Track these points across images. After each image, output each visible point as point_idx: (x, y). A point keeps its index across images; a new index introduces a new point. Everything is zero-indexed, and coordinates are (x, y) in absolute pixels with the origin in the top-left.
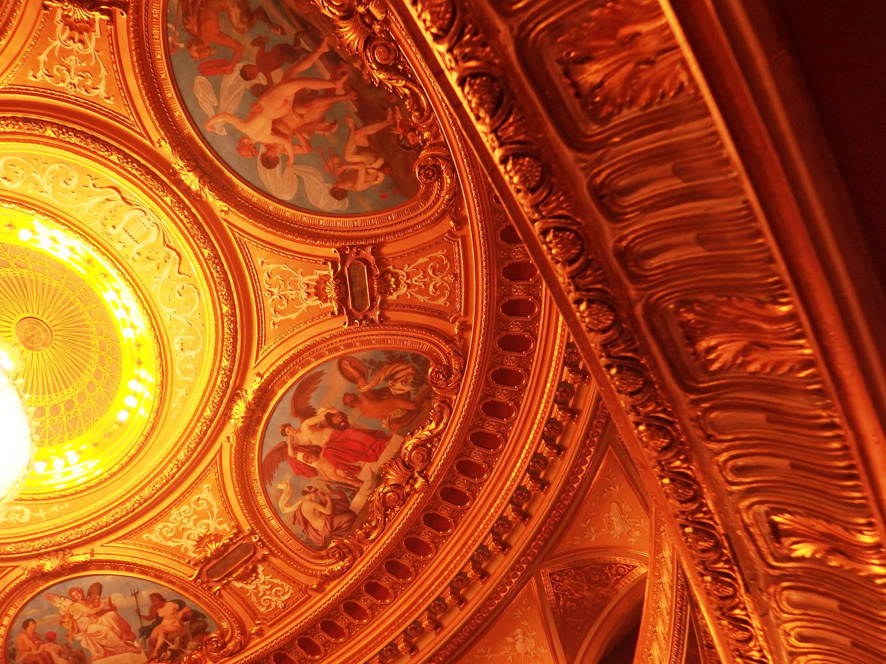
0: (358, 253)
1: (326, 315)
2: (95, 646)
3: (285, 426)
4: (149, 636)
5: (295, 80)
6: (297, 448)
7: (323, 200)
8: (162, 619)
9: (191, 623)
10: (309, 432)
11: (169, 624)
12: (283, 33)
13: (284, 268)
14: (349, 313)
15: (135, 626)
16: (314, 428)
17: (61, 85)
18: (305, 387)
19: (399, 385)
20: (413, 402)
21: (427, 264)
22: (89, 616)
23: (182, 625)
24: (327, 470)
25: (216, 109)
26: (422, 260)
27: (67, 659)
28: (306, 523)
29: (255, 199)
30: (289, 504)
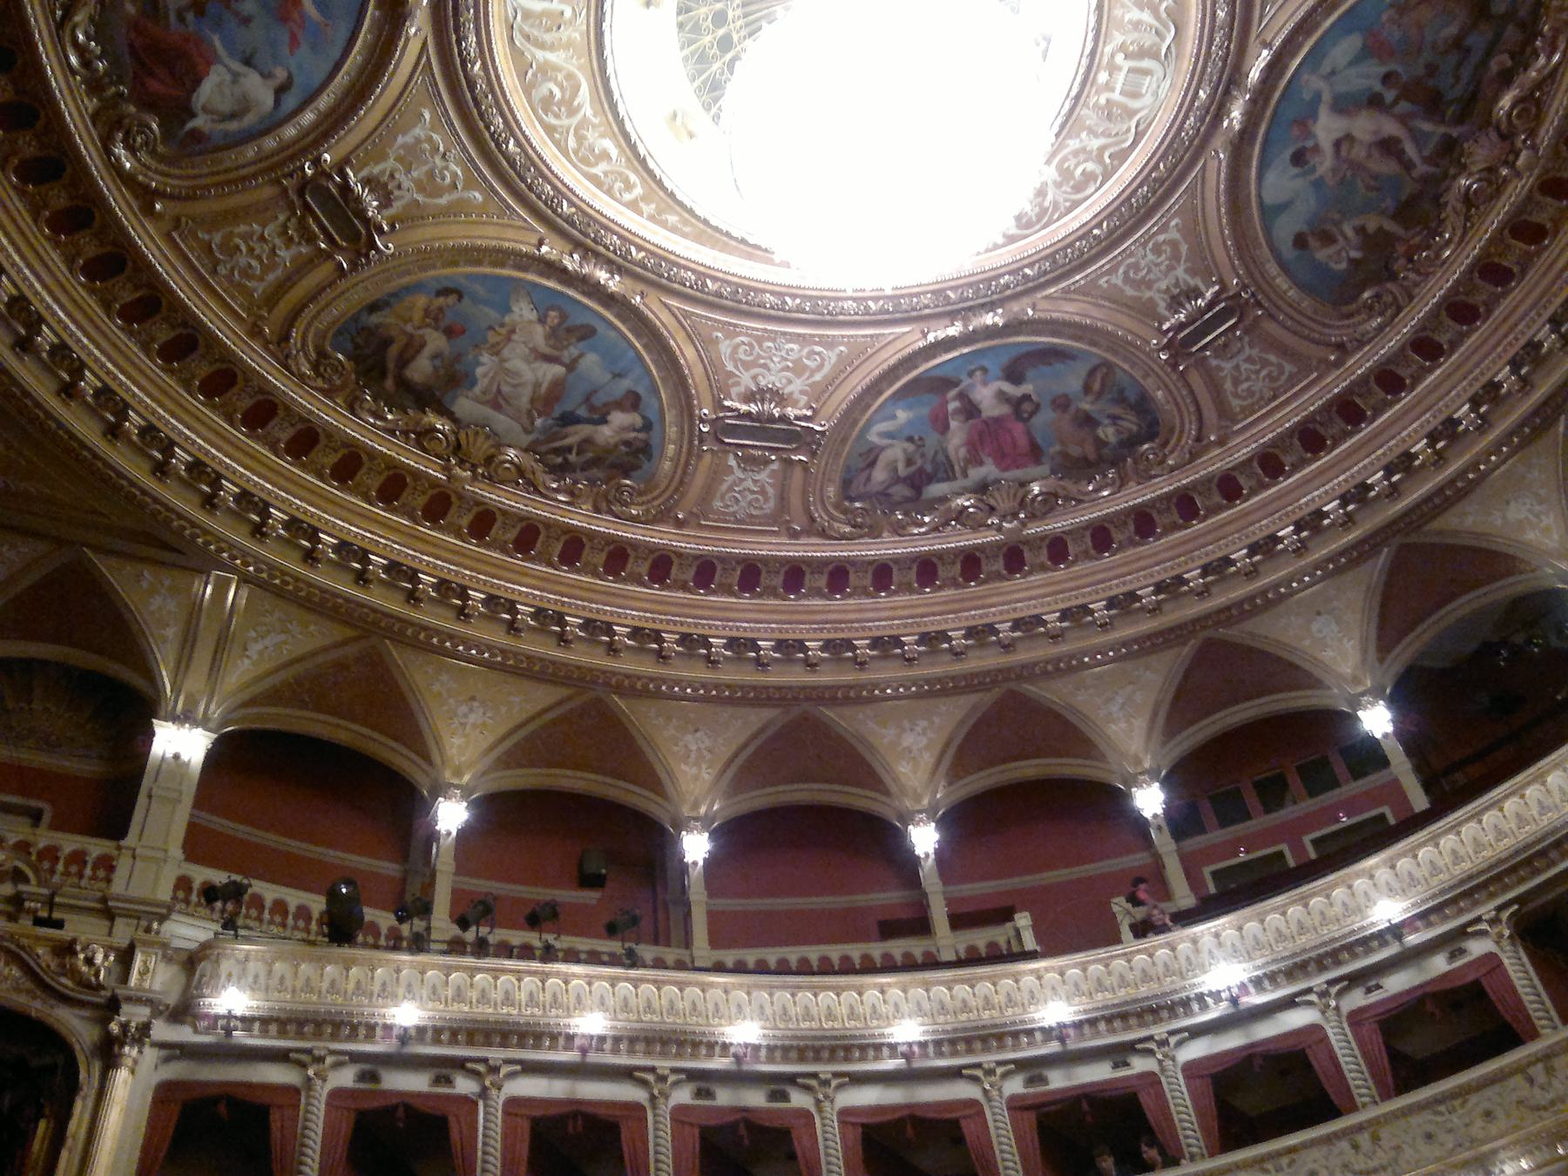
2: (491, 383)
3: (984, 370)
6: (962, 396)
12: (1452, 86)
14: (1171, 340)
16: (1002, 396)
21: (1271, 364)
23: (616, 446)
24: (957, 438)
26: (1272, 358)
28: (872, 464)
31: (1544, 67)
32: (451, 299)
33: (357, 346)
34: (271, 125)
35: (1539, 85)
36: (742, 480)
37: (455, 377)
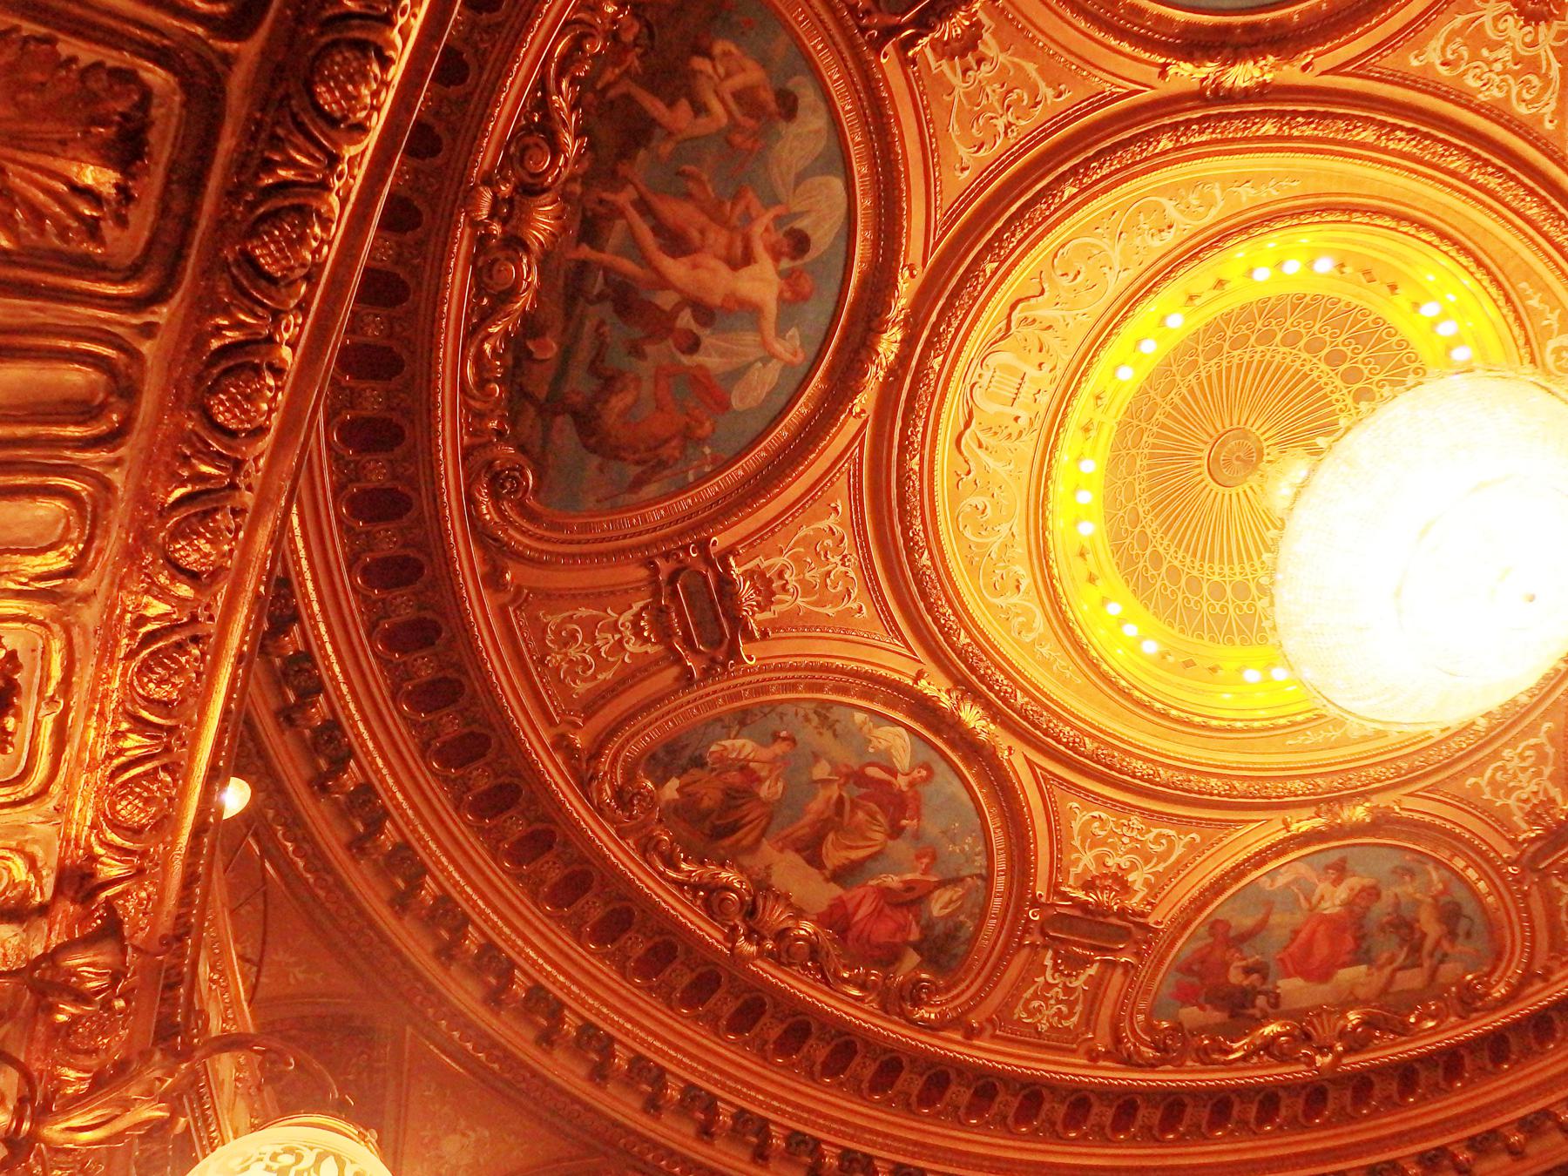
0: (868, 13)
1: (1003, 9)
5: (656, 270)
7: (812, 122)
12: (602, 323)
13: (955, 130)
17: (852, 574)
25: (765, 361)
29: (868, 235)
31: (482, 342)
35: (487, 317)
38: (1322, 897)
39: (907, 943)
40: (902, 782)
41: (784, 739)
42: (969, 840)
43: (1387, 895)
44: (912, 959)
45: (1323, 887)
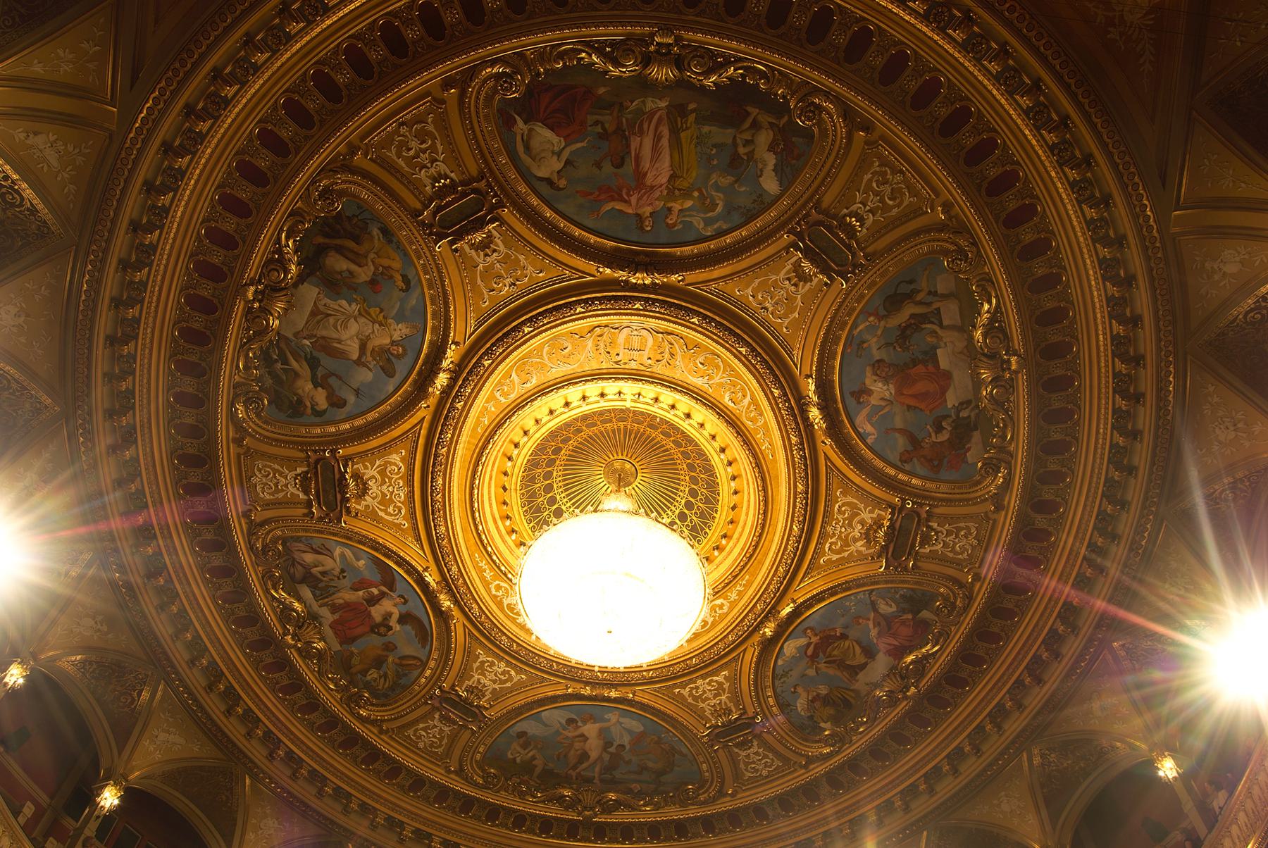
2: (334, 310)
3: (406, 602)
4: (306, 360)
5: (597, 760)
6: (383, 595)
8: (316, 387)
9: (291, 402)
10: (388, 610)
11: (305, 386)
15: (327, 362)
16: (388, 616)
18: (423, 635)
19: (375, 675)
20: (356, 674)
22: (368, 338)
23: (296, 394)
25: (621, 723)
27: (340, 273)
30: (343, 555)
32: (401, 284)
33: (349, 219)
34: (526, 175)
36: (286, 477)
37: (334, 285)
38: (882, 399)
39: (913, 619)
40: (814, 640)
41: (795, 689)
42: (847, 604)
43: (877, 355)
44: (925, 614)
45: (874, 400)
